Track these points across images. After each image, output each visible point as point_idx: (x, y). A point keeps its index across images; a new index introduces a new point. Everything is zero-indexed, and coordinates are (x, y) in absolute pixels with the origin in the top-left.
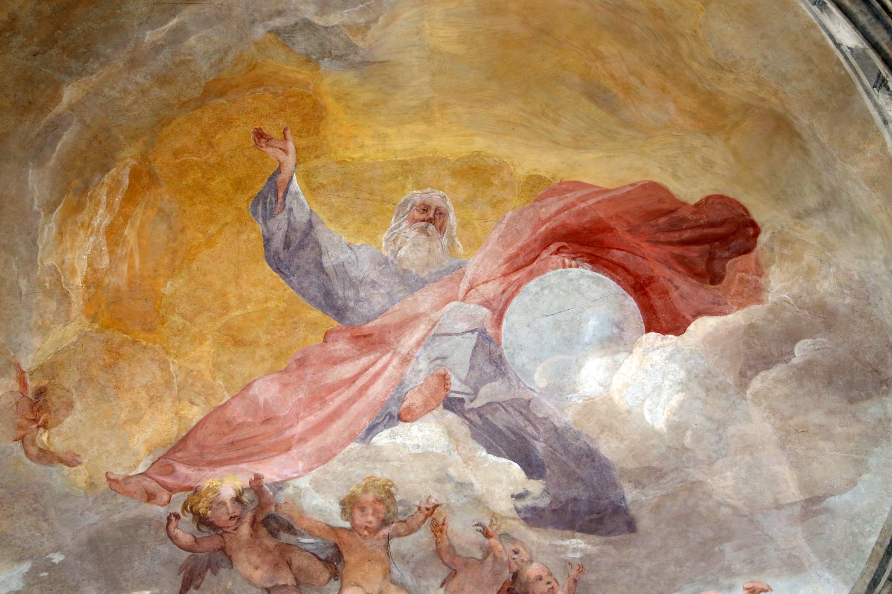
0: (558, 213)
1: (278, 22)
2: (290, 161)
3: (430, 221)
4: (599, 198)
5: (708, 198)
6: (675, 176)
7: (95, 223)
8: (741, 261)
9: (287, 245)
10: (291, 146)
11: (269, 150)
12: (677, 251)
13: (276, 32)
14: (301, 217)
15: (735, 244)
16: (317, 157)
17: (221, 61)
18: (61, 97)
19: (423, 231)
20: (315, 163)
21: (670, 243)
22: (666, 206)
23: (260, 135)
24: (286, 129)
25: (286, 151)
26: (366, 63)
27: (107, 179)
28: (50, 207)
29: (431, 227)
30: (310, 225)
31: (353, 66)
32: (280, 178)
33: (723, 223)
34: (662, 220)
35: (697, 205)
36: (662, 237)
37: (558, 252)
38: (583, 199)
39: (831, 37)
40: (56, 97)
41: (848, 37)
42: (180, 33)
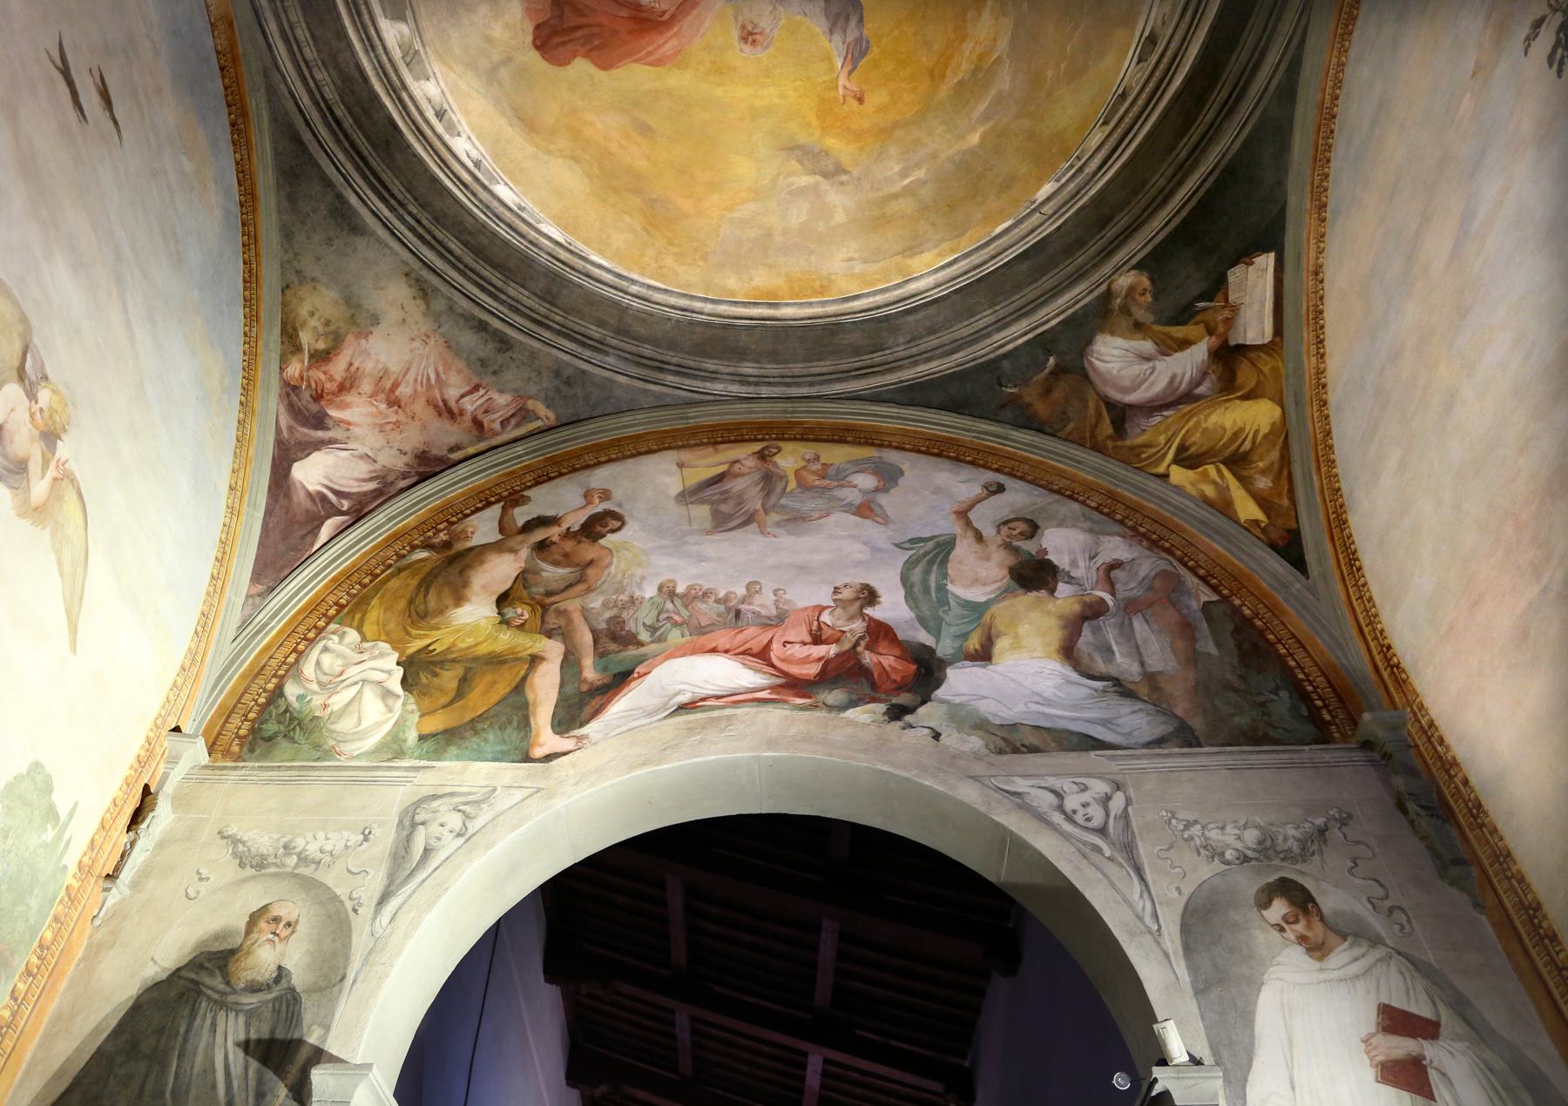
0: (666, 42)
1: (844, 178)
2: (842, 81)
3: (751, 34)
4: (639, 55)
5: (569, 63)
6: (591, 76)
7: (972, 44)
8: (543, 18)
9: (847, 18)
10: (841, 91)
11: (855, 89)
12: (585, 21)
13: (845, 172)
14: (837, 38)
15: (546, 31)
16: (824, 82)
17: (881, 153)
18: (980, 138)
19: (755, 26)
20: (827, 78)
21: (591, 26)
22: (595, 53)
23: (861, 100)
24: (844, 103)
25: (845, 87)
26: (792, 149)
27: (961, 75)
28: (999, 60)
29: (750, 28)
30: (831, 32)
31: (799, 147)
32: (850, 67)
33: (557, 45)
34: (596, 43)
35: (575, 57)
36: (595, 30)
37: (664, 12)
38: (650, 53)
39: (511, 189)
40: (984, 137)
41: (501, 190)
42: (904, 174)
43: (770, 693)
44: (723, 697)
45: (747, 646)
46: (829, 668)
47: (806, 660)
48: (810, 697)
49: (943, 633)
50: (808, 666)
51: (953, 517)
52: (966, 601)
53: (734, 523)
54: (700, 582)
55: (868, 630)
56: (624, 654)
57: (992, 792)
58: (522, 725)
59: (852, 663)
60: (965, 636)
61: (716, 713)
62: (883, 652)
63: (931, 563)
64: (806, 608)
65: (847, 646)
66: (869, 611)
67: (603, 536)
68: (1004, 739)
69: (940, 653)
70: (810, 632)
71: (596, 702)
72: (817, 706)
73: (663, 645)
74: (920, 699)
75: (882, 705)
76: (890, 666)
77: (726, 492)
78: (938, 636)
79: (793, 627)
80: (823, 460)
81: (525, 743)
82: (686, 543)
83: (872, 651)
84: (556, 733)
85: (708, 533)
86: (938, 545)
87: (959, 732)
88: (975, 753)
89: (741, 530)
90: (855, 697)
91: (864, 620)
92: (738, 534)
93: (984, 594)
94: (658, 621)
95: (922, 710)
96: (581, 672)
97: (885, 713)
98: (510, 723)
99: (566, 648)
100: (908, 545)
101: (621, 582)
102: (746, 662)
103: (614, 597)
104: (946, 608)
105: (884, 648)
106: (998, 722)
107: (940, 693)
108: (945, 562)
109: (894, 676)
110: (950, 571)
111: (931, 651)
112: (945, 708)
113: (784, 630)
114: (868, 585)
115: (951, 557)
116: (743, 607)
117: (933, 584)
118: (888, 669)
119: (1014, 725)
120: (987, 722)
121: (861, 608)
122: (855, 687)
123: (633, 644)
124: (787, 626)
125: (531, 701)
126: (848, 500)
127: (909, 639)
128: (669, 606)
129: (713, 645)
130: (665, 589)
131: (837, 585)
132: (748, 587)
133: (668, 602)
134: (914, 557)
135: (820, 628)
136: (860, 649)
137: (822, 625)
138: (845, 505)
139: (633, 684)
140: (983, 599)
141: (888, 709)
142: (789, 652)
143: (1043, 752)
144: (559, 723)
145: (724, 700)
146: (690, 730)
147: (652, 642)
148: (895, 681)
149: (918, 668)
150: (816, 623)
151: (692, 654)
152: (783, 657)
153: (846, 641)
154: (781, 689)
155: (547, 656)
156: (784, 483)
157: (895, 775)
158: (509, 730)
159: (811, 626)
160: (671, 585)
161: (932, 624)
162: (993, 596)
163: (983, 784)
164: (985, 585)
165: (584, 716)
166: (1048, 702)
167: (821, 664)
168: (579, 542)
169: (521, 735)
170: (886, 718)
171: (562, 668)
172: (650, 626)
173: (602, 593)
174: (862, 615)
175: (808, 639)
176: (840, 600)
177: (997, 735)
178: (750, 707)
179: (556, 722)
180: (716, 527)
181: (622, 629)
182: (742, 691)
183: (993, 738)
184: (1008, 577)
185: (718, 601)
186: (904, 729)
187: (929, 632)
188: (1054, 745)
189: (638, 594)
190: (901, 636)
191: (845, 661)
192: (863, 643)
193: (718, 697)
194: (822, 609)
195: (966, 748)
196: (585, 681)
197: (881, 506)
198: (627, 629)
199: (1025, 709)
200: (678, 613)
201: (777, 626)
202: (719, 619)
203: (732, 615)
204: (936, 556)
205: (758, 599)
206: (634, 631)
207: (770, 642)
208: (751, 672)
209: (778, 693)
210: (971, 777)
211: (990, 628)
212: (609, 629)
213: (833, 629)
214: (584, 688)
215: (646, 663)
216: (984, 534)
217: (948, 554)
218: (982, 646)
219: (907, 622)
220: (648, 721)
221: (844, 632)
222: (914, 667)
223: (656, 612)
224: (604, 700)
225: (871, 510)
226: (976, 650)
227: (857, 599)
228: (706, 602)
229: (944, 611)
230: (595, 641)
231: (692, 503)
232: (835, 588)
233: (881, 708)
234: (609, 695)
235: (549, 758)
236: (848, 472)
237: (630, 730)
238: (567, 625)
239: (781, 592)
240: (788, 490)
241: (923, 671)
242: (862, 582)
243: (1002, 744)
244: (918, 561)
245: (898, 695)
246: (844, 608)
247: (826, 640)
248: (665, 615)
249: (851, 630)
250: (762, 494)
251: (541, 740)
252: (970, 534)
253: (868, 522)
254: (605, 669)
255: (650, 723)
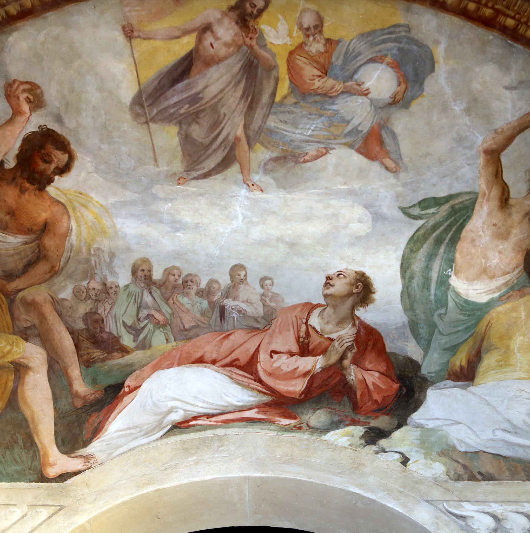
43: (258, 413)
44: (214, 415)
45: (234, 356)
46: (315, 385)
47: (292, 375)
48: (295, 418)
49: (432, 345)
50: (294, 382)
51: (481, 160)
52: (467, 302)
53: (210, 164)
54: (178, 264)
55: (357, 339)
56: (110, 363)
57: (442, 515)
58: (28, 444)
59: (338, 379)
60: (453, 349)
61: (209, 433)
62: (369, 366)
63: (439, 242)
64: (295, 307)
65: (334, 358)
66: (360, 313)
67: (50, 181)
68: (465, 467)
69: (424, 371)
70: (298, 341)
71: (94, 419)
72: (300, 428)
73: (148, 353)
74: (396, 422)
75: (361, 428)
76: (374, 384)
77: (195, 99)
78: (426, 349)
79: (280, 332)
80: (327, 33)
81: (36, 463)
82: (155, 198)
83: (358, 366)
84: (63, 453)
85: (180, 180)
86: (454, 211)
87: (425, 458)
88: (435, 479)
89: (219, 176)
90: (336, 418)
91: (354, 325)
92: (215, 181)
93: (487, 292)
94: (139, 320)
95: (397, 434)
96: (71, 385)
97: (362, 437)
98: (16, 442)
99: (48, 354)
100: (417, 211)
101: (88, 261)
102: (234, 376)
103: (85, 283)
104: (443, 311)
105: (370, 362)
106: (463, 449)
107: (416, 417)
108: (455, 240)
109: (377, 397)
110: (458, 256)
111: (415, 366)
112: (417, 433)
113: (271, 336)
114: (363, 275)
115: (464, 233)
116: (229, 303)
117: (434, 275)
118: (371, 387)
119: (478, 452)
120: (454, 448)
121: (353, 308)
122: (337, 407)
123: (117, 350)
124: (274, 331)
125: (30, 420)
126: (355, 122)
127: (397, 352)
128: (148, 299)
129: (199, 355)
130: (140, 273)
131: (331, 272)
132: (232, 276)
133: (146, 293)
134: (422, 231)
135: (308, 334)
136: (346, 362)
137: (311, 331)
138: (350, 133)
139: (126, 399)
140: (484, 299)
141: (366, 432)
142: (276, 365)
143: (495, 480)
144: (63, 442)
145: (214, 419)
146: (186, 450)
147: (137, 348)
148: (376, 401)
149: (400, 388)
150: (304, 327)
151: (179, 364)
152: (269, 370)
153: (333, 353)
154: (267, 409)
155: (30, 365)
156: (272, 82)
157: (363, 497)
158: (17, 450)
159: (298, 332)
160: (146, 268)
161: (423, 332)
162: (496, 295)
163: (436, 507)
164: (492, 278)
165: (85, 434)
166: (515, 430)
167: (306, 380)
168: (23, 191)
169: (30, 455)
170: (363, 441)
171: (50, 379)
172: (130, 327)
173: (70, 276)
174: (353, 317)
175: (295, 348)
176: (331, 295)
177: (458, 462)
178: (239, 427)
179: (60, 442)
180: (189, 169)
181: (102, 330)
182: (231, 409)
183: (456, 464)
184: (522, 267)
185: (200, 293)
186: (377, 453)
187: (418, 343)
188: (507, 473)
189: (110, 280)
190: (390, 346)
191: (330, 377)
192: (350, 355)
193: (209, 416)
194: (310, 307)
195: (428, 474)
196: (76, 395)
197: (394, 136)
198: (107, 330)
199: (491, 437)
200: (159, 311)
201: (264, 330)
202: (203, 319)
203: (217, 314)
204: (450, 226)
205: (243, 292)
206: (114, 332)
207: (257, 350)
208: (240, 387)
209: (265, 413)
210: (428, 501)
211: (482, 340)
212: (88, 330)
213: (321, 335)
214: (79, 403)
215: (134, 375)
216: (512, 195)
217: (462, 227)
218: (469, 362)
219: (397, 329)
220: (145, 440)
221: (332, 340)
222: (396, 386)
223: (135, 308)
224: (101, 418)
225: (381, 143)
226: (461, 367)
227: (350, 294)
228: (187, 295)
229: (440, 315)
230: (77, 346)
231: (153, 120)
232: (328, 278)
233: (359, 430)
234: (104, 411)
235: (63, 477)
236: (362, 59)
237: (130, 450)
238: (41, 322)
239: (268, 282)
240: (278, 99)
241: (404, 391)
242: (358, 269)
243: (461, 471)
244: (425, 237)
245: (377, 417)
246: (335, 307)
247: (314, 349)
248: (144, 313)
249: (340, 338)
250: (243, 106)
251: (51, 460)
252: (495, 193)
253: (376, 166)
254: (94, 382)
255: (149, 443)
